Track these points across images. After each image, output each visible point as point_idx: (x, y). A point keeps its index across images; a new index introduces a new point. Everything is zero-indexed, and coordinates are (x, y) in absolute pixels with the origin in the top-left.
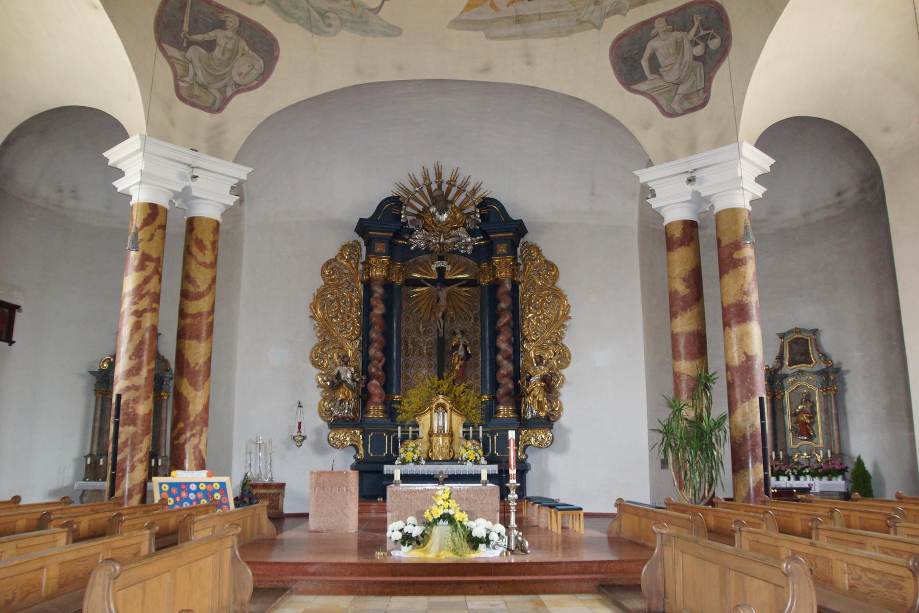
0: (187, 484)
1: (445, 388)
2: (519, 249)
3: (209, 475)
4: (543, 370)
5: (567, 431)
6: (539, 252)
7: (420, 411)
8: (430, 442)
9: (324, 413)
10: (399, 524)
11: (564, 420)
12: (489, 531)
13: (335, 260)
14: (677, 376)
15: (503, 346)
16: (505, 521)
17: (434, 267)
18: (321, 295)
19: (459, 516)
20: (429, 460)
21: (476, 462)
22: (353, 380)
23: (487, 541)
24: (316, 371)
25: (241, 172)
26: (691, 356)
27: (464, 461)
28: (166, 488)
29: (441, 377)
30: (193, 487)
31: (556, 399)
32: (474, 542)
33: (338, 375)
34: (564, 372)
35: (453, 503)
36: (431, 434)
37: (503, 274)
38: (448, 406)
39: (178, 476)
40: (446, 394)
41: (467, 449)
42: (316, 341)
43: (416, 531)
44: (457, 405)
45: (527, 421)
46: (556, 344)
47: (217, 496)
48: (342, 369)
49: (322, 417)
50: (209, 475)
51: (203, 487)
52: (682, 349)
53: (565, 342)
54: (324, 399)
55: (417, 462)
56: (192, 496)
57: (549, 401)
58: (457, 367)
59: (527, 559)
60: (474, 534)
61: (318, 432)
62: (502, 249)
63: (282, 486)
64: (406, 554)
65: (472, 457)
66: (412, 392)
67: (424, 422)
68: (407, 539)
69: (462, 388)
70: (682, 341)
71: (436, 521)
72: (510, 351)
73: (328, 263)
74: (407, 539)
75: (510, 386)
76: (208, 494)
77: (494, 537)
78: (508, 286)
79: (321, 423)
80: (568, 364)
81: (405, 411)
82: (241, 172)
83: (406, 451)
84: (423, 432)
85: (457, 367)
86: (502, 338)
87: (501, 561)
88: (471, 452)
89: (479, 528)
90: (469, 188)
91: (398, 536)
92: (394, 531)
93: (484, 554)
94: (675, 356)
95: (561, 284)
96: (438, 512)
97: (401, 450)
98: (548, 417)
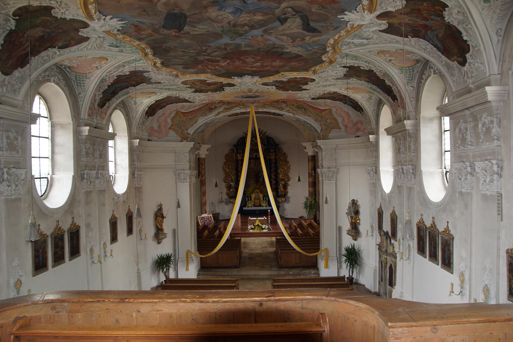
0: (204, 217)
1: (258, 187)
2: (277, 149)
3: (208, 215)
4: (283, 183)
5: (289, 197)
6: (282, 150)
7: (252, 193)
8: (255, 201)
9: (228, 194)
10: (250, 226)
11: (289, 195)
12: (265, 227)
13: (228, 154)
14: (309, 191)
15: (273, 176)
16: (268, 225)
17: (254, 155)
18: (225, 164)
19: (260, 225)
20: (254, 206)
21: (266, 206)
22: (234, 186)
23: (265, 229)
24: (225, 184)
25: (209, 146)
26: (312, 187)
27: (263, 206)
28: (200, 218)
29: (257, 184)
30: (205, 218)
31: (287, 189)
32: (263, 229)
33: (231, 185)
34: (289, 182)
35: (259, 222)
36: (254, 199)
37: (272, 157)
38: (259, 192)
39: (203, 215)
40: (258, 189)
41: (264, 203)
42: (224, 176)
43: (253, 227)
44: (261, 192)
45: (279, 195)
46: (286, 175)
47: (210, 219)
48: (232, 183)
49: (227, 195)
50: (208, 215)
51: (207, 217)
52: (310, 186)
53: (289, 175)
54: (227, 191)
55: (251, 207)
56: (205, 219)
57: (285, 190)
58: (261, 181)
59: (271, 232)
60: (263, 227)
61: (226, 199)
62: (272, 150)
63: (219, 214)
64: (251, 231)
65: (265, 205)
66: (250, 188)
67: (253, 196)
68: (252, 229)
69: (262, 187)
70: (310, 183)
71: (256, 226)
72: (274, 178)
73: (226, 155)
74: (252, 229)
75: (275, 187)
76: (208, 219)
77: (266, 228)
78: (274, 161)
79: (226, 197)
80: (289, 181)
81: (248, 193)
82: (209, 146)
83: (249, 204)
84: (253, 199)
85: (261, 181)
86: (272, 174)
87: (268, 232)
88: (265, 204)
89: (264, 226)
90: (264, 132)
91: (250, 228)
92: (249, 227)
93: (265, 231)
94: (309, 187)
95: (288, 159)
96: (257, 224)
97: (247, 204)
98: (284, 195)
